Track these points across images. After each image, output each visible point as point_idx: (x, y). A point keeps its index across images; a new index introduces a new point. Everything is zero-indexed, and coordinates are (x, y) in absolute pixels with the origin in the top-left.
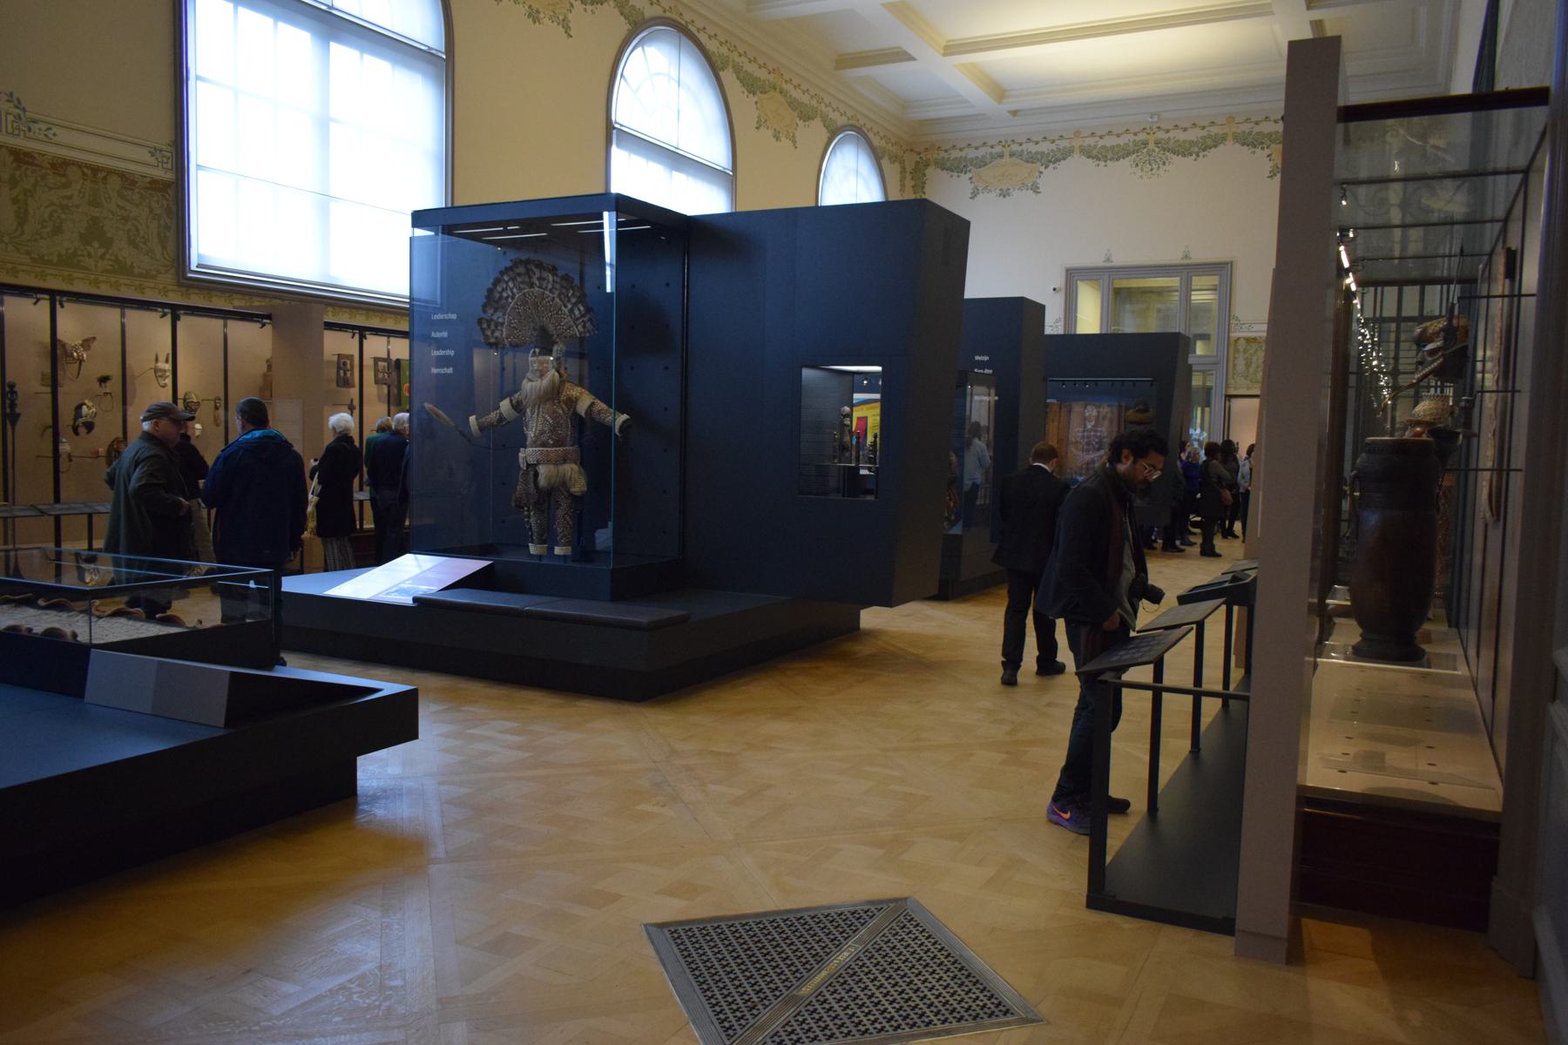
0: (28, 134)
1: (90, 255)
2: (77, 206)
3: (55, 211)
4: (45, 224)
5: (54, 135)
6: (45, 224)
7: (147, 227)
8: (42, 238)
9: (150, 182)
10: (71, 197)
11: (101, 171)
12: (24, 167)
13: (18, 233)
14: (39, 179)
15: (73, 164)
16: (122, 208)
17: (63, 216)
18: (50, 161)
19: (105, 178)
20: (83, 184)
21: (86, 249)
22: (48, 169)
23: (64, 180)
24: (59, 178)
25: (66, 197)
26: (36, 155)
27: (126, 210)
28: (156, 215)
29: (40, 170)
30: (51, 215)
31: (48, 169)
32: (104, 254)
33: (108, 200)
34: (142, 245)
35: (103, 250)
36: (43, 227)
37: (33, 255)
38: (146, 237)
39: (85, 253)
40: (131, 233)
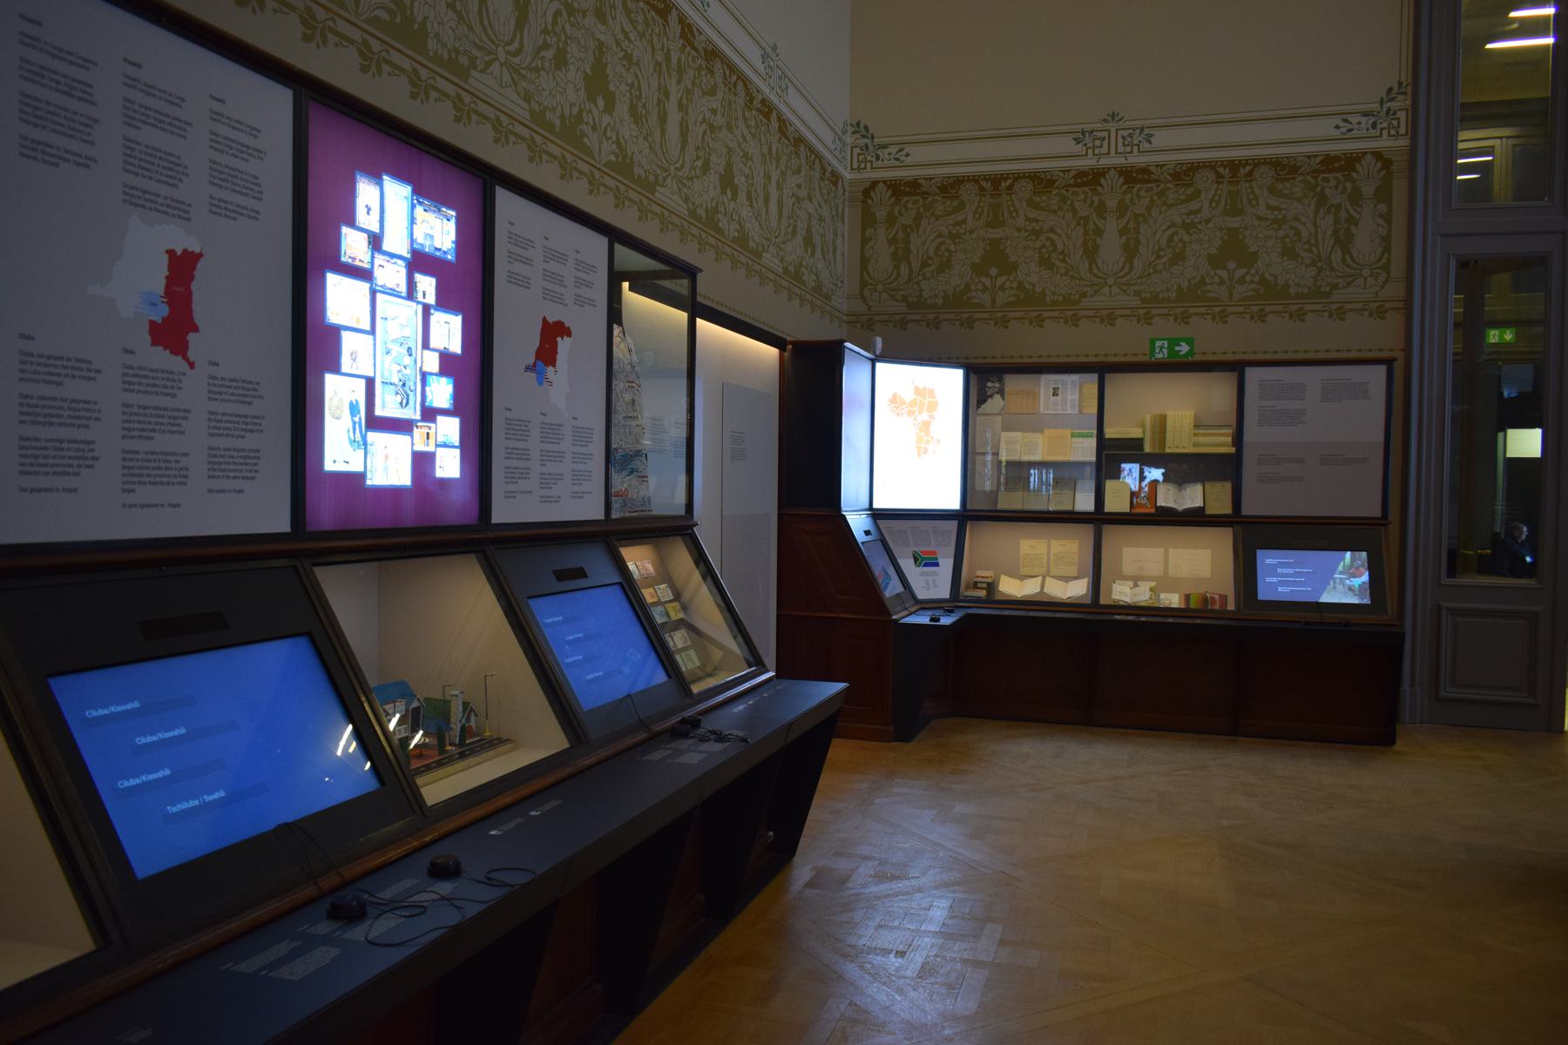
0: (1143, 147)
1: (985, 288)
2: (1208, 221)
3: (1176, 233)
4: (1162, 253)
5: (1337, 127)
6: (1162, 253)
7: (1316, 227)
8: (1156, 271)
9: (1075, 177)
10: (1199, 211)
11: (1005, 180)
12: (905, 199)
13: (1126, 270)
14: (1155, 198)
15: (968, 180)
16: (1273, 208)
17: (1186, 238)
18: (1172, 172)
19: (1010, 188)
20: (1217, 190)
21: (1216, 274)
22: (1169, 181)
23: (1190, 191)
24: (949, 203)
25: (1191, 212)
26: (1151, 168)
27: (1280, 210)
28: (1332, 205)
29: (1158, 186)
30: (1170, 239)
31: (1169, 181)
32: (1243, 277)
33: (1254, 202)
34: (1303, 254)
35: (1243, 271)
36: (1159, 257)
37: (1143, 295)
38: (1313, 241)
39: (1217, 279)
40: (1287, 240)
